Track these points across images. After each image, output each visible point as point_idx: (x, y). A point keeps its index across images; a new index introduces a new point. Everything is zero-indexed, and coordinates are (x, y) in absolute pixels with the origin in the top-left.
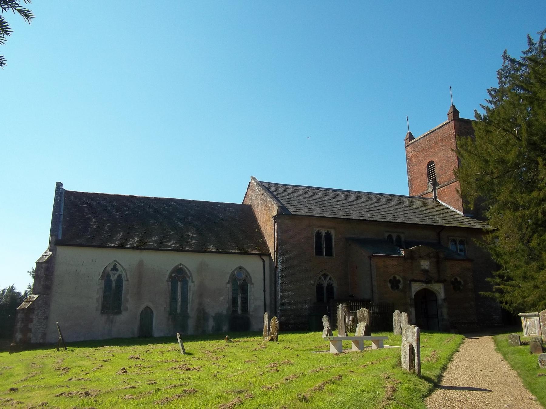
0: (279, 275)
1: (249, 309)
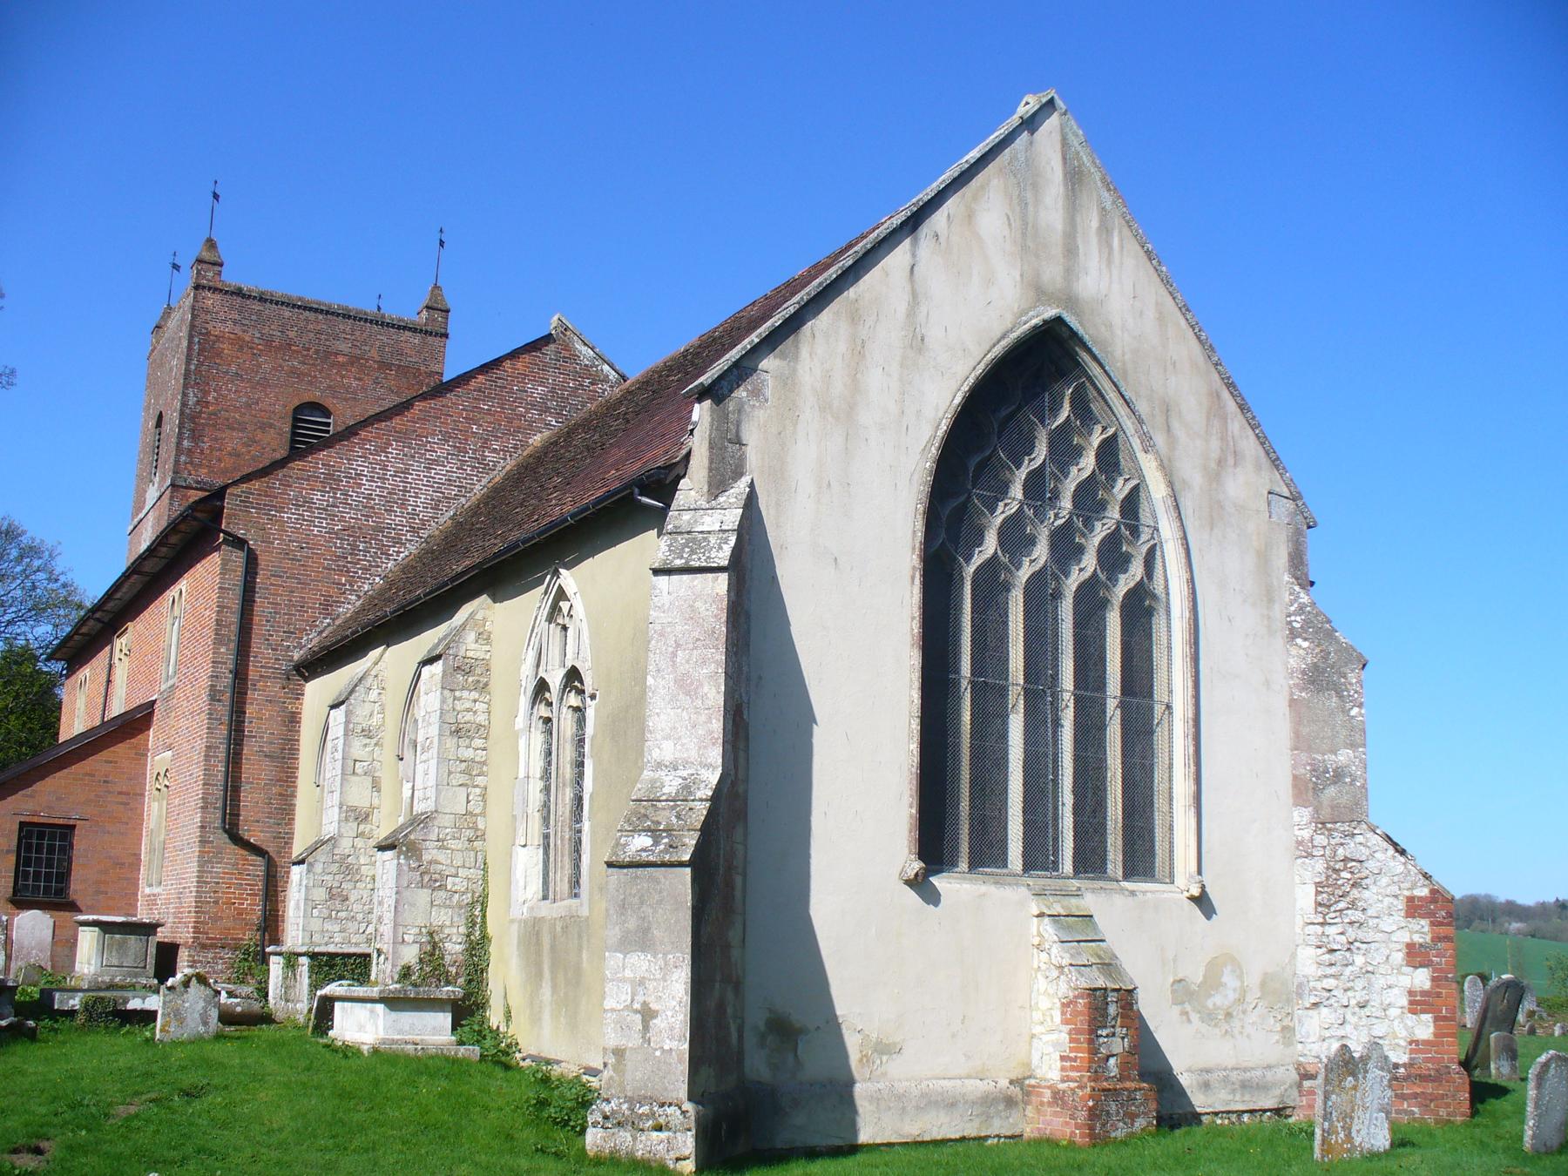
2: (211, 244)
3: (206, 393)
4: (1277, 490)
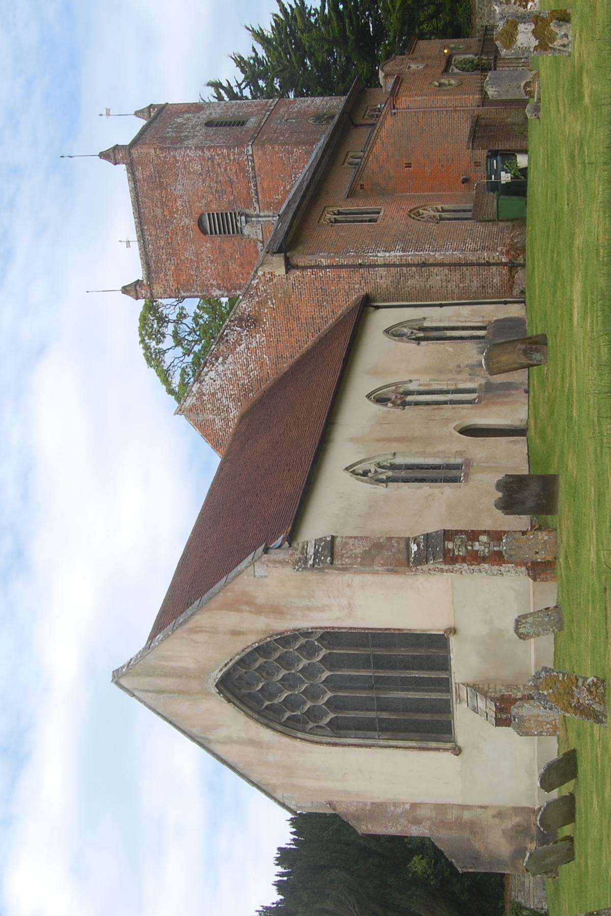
0: (410, 253)
1: (477, 322)
2: (125, 290)
3: (212, 285)
4: (252, 572)
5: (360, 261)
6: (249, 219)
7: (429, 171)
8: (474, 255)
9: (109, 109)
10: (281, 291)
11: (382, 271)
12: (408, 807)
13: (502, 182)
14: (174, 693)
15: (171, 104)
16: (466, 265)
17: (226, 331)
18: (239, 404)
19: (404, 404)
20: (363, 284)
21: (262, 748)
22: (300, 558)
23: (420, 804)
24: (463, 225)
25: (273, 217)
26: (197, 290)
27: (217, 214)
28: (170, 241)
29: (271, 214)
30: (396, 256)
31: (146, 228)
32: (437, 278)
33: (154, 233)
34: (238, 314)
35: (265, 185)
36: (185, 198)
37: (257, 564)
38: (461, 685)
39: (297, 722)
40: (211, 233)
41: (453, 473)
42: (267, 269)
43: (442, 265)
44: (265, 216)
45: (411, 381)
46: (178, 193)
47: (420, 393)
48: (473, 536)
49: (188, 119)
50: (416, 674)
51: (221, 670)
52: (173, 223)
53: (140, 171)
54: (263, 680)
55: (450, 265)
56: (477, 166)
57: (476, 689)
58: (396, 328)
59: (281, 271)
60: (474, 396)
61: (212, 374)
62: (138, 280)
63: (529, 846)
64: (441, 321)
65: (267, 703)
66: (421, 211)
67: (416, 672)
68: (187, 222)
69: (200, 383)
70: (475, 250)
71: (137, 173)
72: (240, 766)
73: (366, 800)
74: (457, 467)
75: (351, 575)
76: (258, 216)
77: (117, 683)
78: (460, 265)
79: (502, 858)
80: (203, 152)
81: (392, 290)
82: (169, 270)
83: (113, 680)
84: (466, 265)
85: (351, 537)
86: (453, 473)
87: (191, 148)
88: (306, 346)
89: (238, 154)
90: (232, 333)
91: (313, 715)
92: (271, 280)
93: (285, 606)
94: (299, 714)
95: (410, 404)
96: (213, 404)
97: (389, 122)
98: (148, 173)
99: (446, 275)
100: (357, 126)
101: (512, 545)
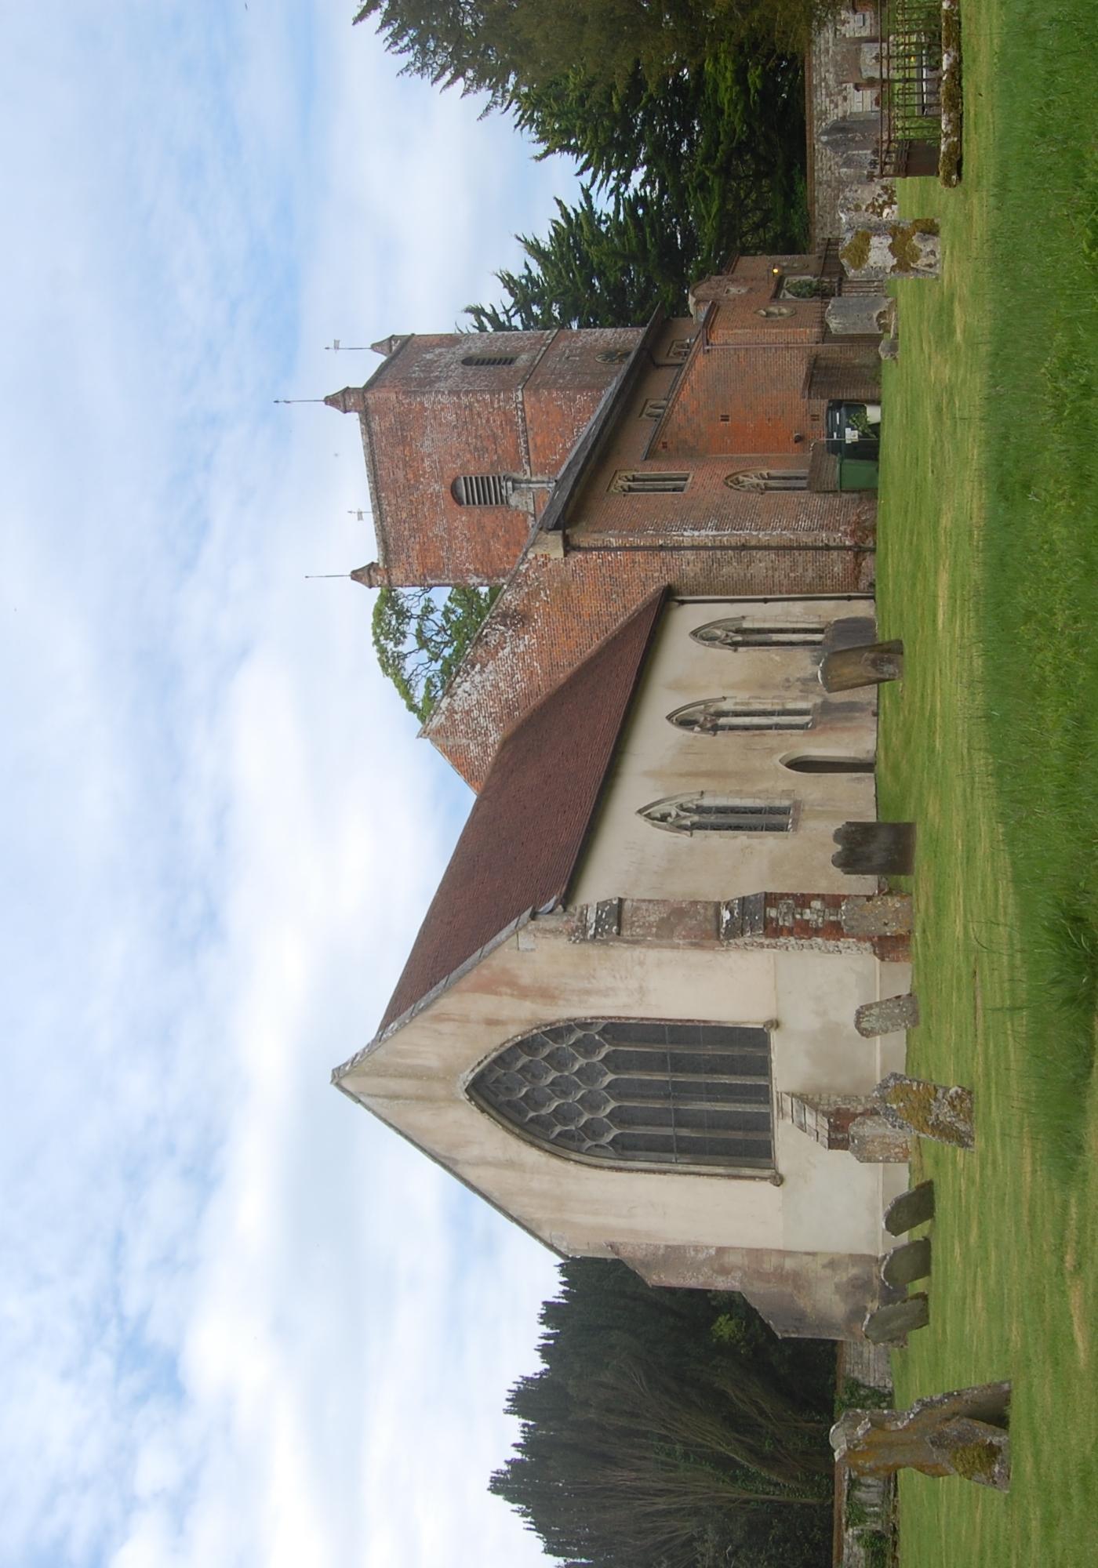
0: (726, 532)
1: (812, 623)
2: (356, 575)
3: (468, 570)
4: (515, 944)
5: (661, 542)
6: (517, 485)
7: (752, 426)
8: (809, 536)
9: (339, 342)
10: (558, 579)
11: (690, 555)
12: (713, 1252)
13: (848, 442)
14: (412, 1099)
15: (419, 336)
16: (799, 548)
17: (485, 631)
18: (501, 725)
19: (716, 728)
20: (664, 572)
21: (524, 1172)
22: (577, 926)
23: (730, 1248)
24: (794, 497)
25: (548, 482)
26: (448, 576)
27: (476, 478)
28: (414, 512)
29: (546, 479)
30: (707, 536)
31: (383, 495)
32: (761, 565)
33: (394, 502)
34: (501, 608)
35: (539, 441)
36: (435, 457)
37: (522, 933)
38: (784, 1095)
39: (570, 1139)
40: (468, 502)
41: (778, 819)
42: (540, 551)
43: (767, 548)
44: (538, 482)
45: (725, 698)
46: (425, 450)
47: (737, 714)
48: (803, 901)
49: (441, 354)
50: (726, 1079)
51: (473, 1070)
52: (418, 489)
53: (377, 422)
54: (527, 1084)
55: (778, 548)
56: (814, 420)
57: (803, 1099)
58: (706, 630)
59: (558, 553)
60: (807, 718)
61: (467, 686)
62: (373, 563)
63: (870, 1305)
64: (764, 621)
65: (532, 1114)
66: (741, 478)
67: (725, 1077)
68: (437, 488)
69: (451, 697)
70: (810, 529)
71: (372, 424)
72: (495, 1195)
73: (658, 1242)
74: (784, 811)
75: (644, 950)
76: (529, 482)
77: (338, 1085)
78: (791, 548)
79: (834, 1321)
80: (459, 397)
81: (701, 579)
82: (413, 550)
83: (332, 1081)
84: (799, 548)
85: (644, 901)
86: (778, 819)
87: (443, 393)
88: (589, 651)
89: (504, 401)
90: (493, 633)
91: (592, 1130)
92: (545, 564)
93: (556, 988)
94: (574, 1128)
95: (723, 728)
96: (467, 725)
97: (701, 361)
98: (387, 425)
99: (772, 562)
100: (659, 366)
101: (853, 914)
